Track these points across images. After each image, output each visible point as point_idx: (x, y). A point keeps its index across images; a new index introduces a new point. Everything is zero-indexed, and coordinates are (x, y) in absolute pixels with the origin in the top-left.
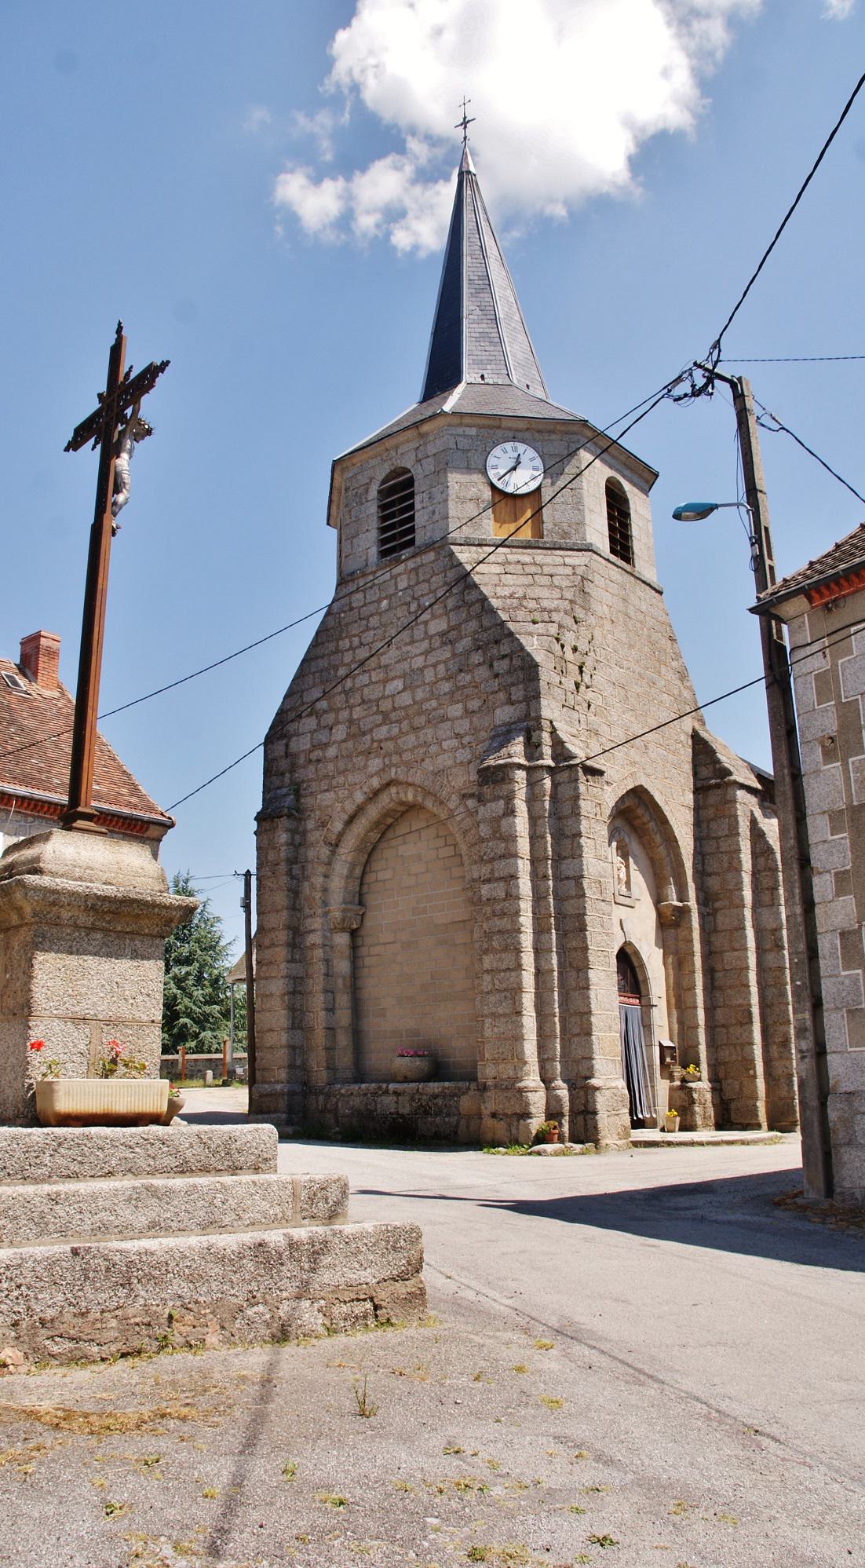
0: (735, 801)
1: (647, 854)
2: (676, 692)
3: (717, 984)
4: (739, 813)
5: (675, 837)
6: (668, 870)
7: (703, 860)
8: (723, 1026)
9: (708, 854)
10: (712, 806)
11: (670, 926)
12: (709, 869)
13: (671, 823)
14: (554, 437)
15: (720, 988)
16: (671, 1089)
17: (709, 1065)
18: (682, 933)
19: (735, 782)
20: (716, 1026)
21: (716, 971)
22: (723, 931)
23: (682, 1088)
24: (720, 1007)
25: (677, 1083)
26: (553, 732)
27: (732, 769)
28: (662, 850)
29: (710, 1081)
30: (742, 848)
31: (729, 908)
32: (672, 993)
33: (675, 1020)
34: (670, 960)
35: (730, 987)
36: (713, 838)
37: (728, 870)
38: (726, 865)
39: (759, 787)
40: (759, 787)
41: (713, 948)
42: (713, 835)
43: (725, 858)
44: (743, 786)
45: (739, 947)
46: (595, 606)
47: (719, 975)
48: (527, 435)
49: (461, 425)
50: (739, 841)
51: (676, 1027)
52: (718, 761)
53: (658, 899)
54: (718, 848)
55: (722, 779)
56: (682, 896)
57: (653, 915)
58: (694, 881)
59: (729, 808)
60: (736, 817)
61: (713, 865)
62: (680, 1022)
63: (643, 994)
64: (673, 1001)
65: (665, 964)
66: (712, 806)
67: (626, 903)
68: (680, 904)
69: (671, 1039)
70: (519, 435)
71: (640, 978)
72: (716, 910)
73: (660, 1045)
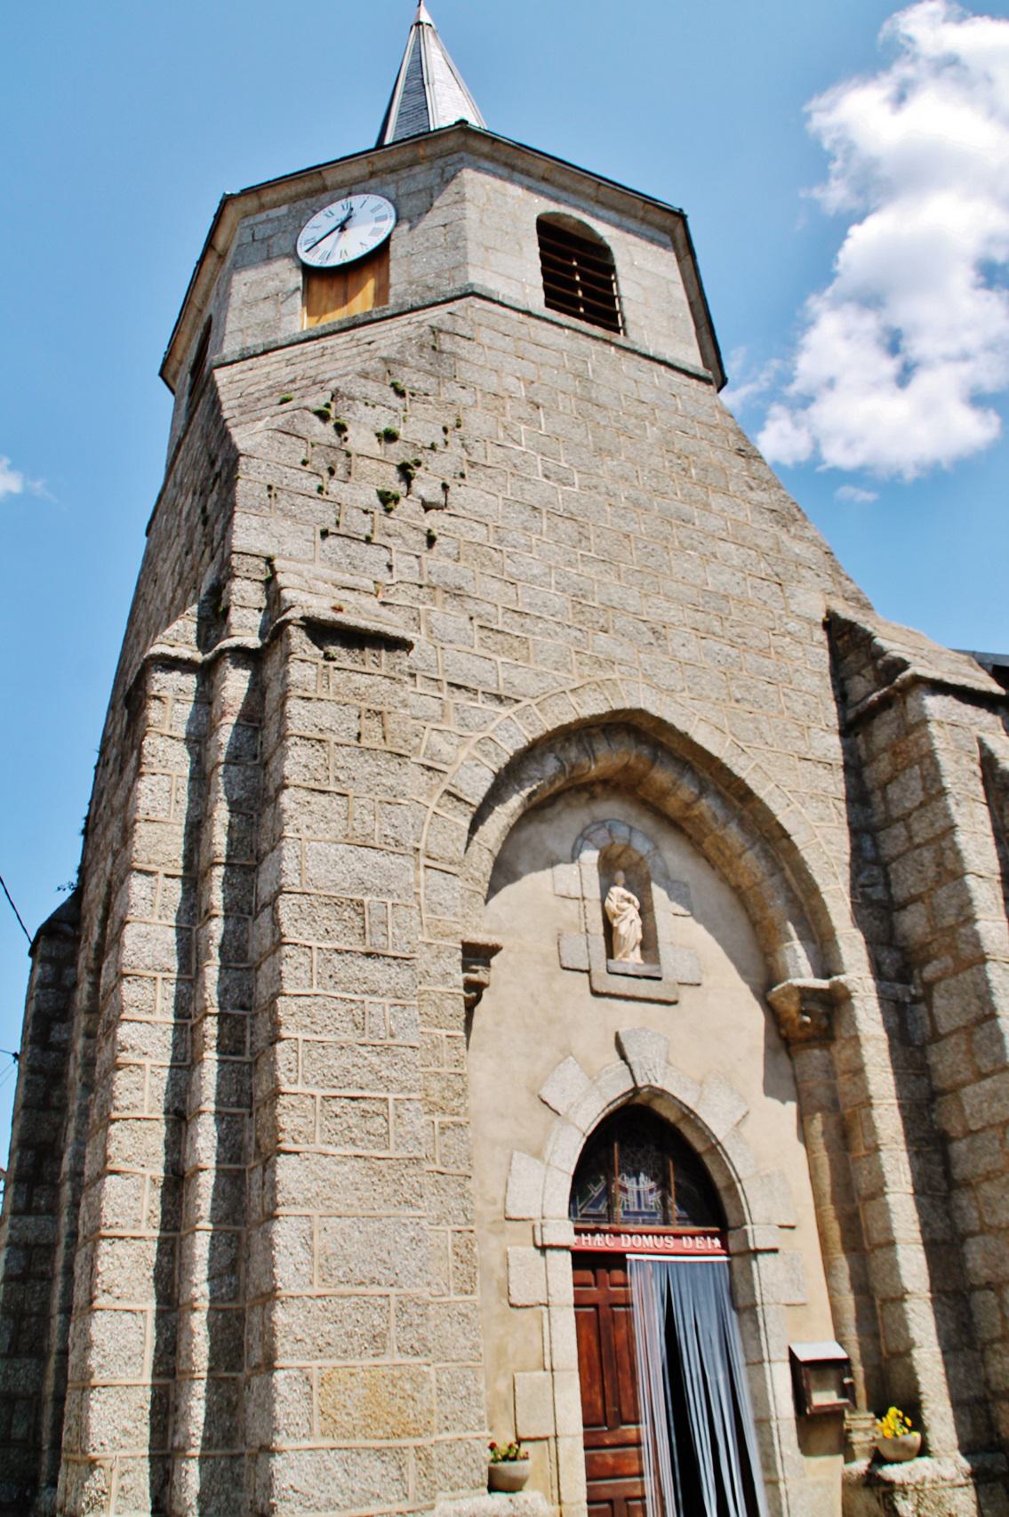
0: (925, 722)
1: (724, 879)
2: (765, 543)
3: (958, 1172)
4: (937, 743)
5: (779, 826)
6: (777, 906)
7: (887, 875)
8: (989, 1286)
9: (893, 859)
10: (884, 750)
11: (808, 1041)
12: (899, 893)
13: (761, 793)
14: (417, 169)
15: (967, 1184)
16: (847, 1484)
17: (957, 1404)
18: (841, 1053)
19: (917, 680)
20: (973, 1288)
21: (952, 1140)
22: (950, 1034)
23: (871, 1480)
24: (973, 1234)
25: (861, 1465)
26: (271, 585)
27: (908, 658)
28: (752, 863)
29: (967, 1449)
30: (958, 820)
31: (956, 973)
32: (830, 1211)
33: (844, 1282)
34: (817, 1124)
35: (988, 1177)
36: (898, 820)
37: (939, 882)
38: (931, 872)
39: (997, 689)
40: (997, 689)
41: (937, 1083)
42: (896, 812)
43: (927, 855)
44: (939, 687)
45: (990, 1067)
46: (466, 373)
47: (959, 1148)
48: (373, 182)
49: (262, 208)
50: (946, 808)
51: (848, 1301)
52: (881, 652)
53: (765, 981)
54: (910, 838)
55: (890, 681)
56: (826, 963)
57: (755, 1019)
58: (859, 920)
59: (916, 743)
60: (931, 754)
61: (907, 881)
62: (863, 1288)
63: (732, 1223)
64: (835, 1231)
65: (804, 1136)
66: (884, 750)
67: (641, 994)
68: (824, 984)
69: (840, 1339)
70: (354, 188)
71: (719, 1180)
72: (929, 986)
73: (793, 1358)
